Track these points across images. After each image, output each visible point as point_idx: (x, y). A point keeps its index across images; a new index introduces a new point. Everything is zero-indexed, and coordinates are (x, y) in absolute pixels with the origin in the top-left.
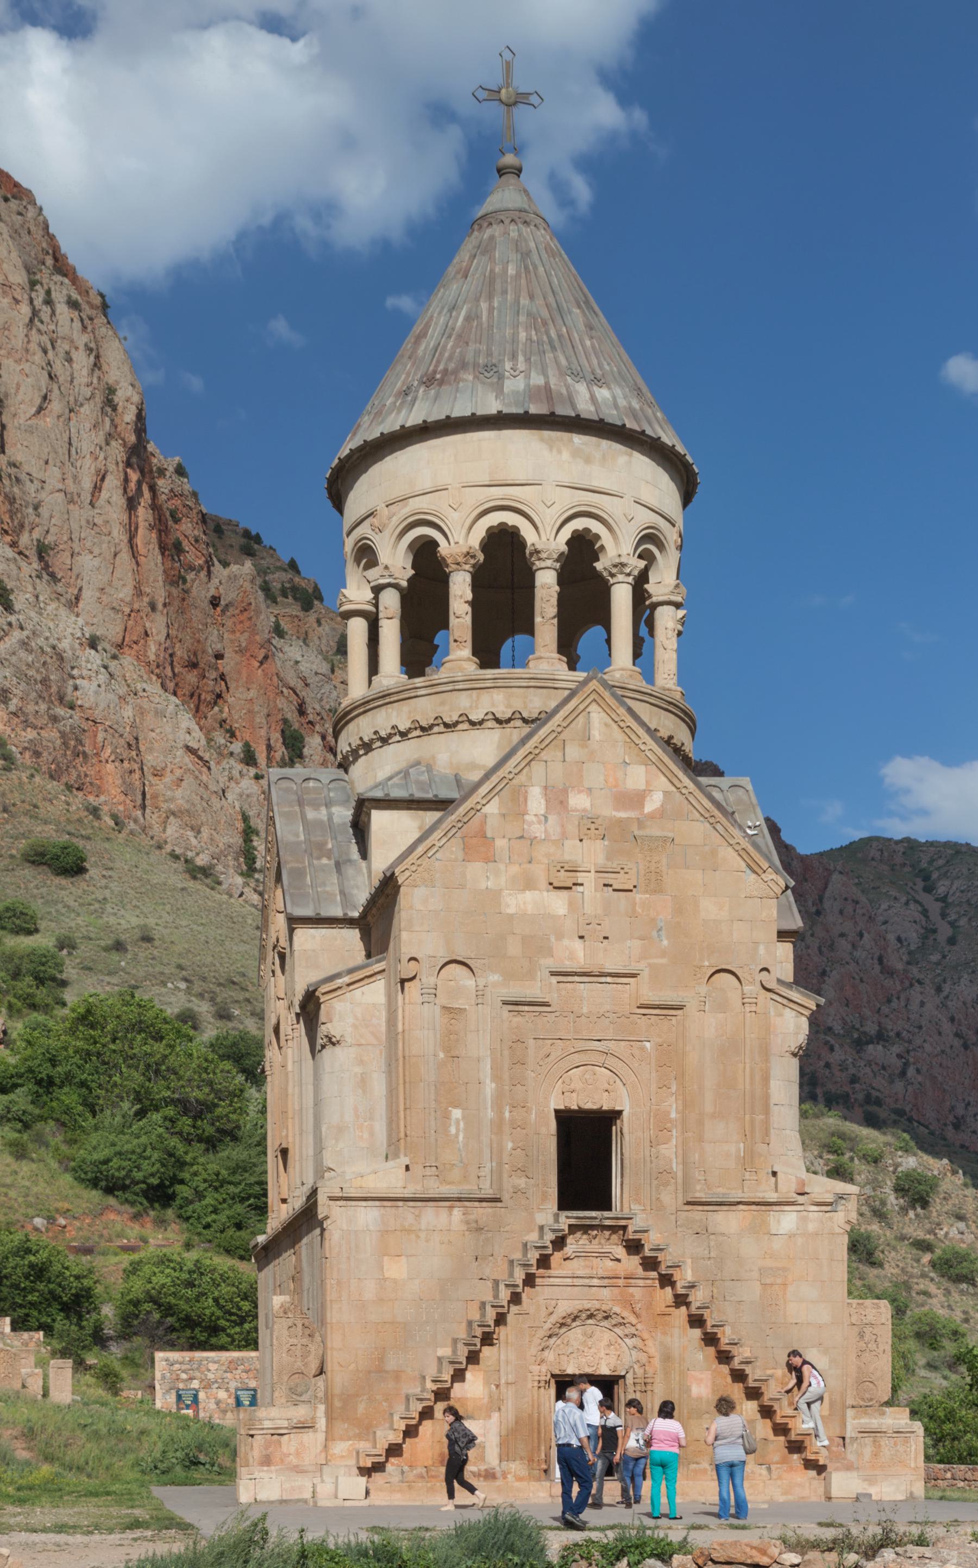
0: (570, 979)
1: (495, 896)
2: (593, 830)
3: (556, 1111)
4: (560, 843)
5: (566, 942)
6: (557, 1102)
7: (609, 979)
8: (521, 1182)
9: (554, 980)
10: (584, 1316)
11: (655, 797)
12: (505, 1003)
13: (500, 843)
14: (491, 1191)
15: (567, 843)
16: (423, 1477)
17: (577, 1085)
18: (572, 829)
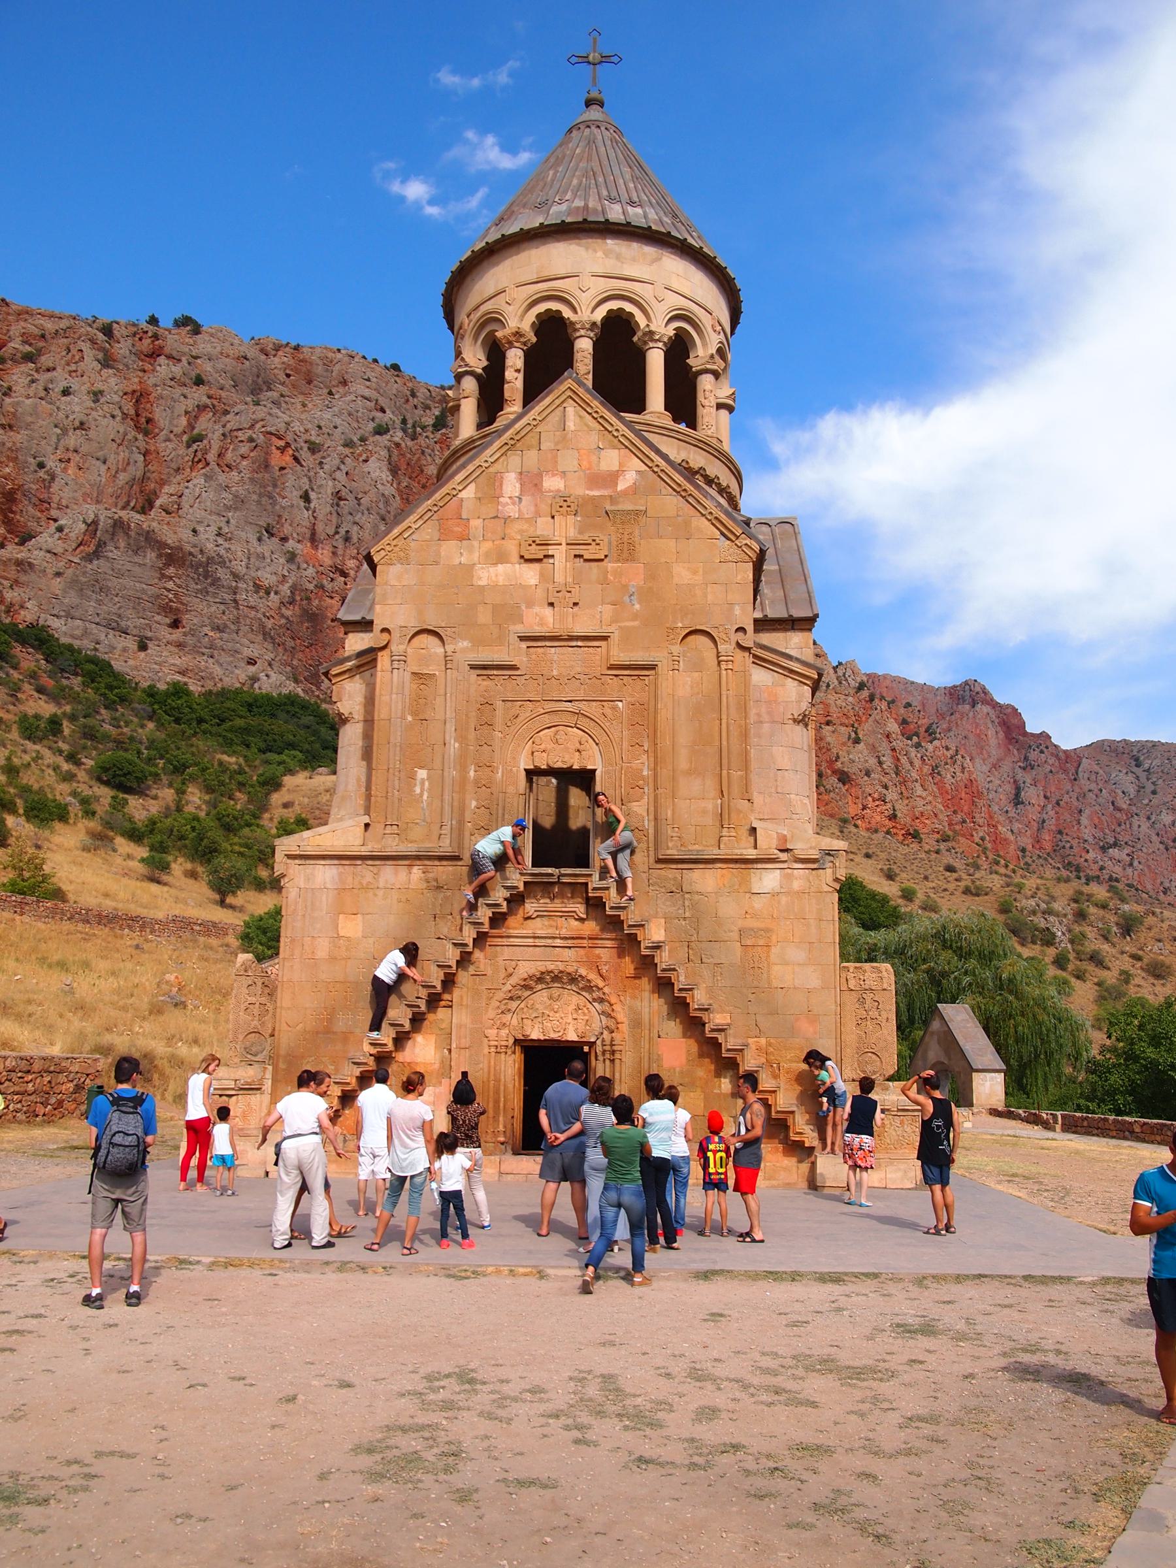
0: (539, 644)
2: (565, 509)
4: (532, 521)
5: (537, 609)
7: (579, 643)
9: (524, 645)
12: (473, 667)
13: (476, 523)
14: (450, 849)
15: (539, 520)
17: (549, 745)
18: (544, 508)
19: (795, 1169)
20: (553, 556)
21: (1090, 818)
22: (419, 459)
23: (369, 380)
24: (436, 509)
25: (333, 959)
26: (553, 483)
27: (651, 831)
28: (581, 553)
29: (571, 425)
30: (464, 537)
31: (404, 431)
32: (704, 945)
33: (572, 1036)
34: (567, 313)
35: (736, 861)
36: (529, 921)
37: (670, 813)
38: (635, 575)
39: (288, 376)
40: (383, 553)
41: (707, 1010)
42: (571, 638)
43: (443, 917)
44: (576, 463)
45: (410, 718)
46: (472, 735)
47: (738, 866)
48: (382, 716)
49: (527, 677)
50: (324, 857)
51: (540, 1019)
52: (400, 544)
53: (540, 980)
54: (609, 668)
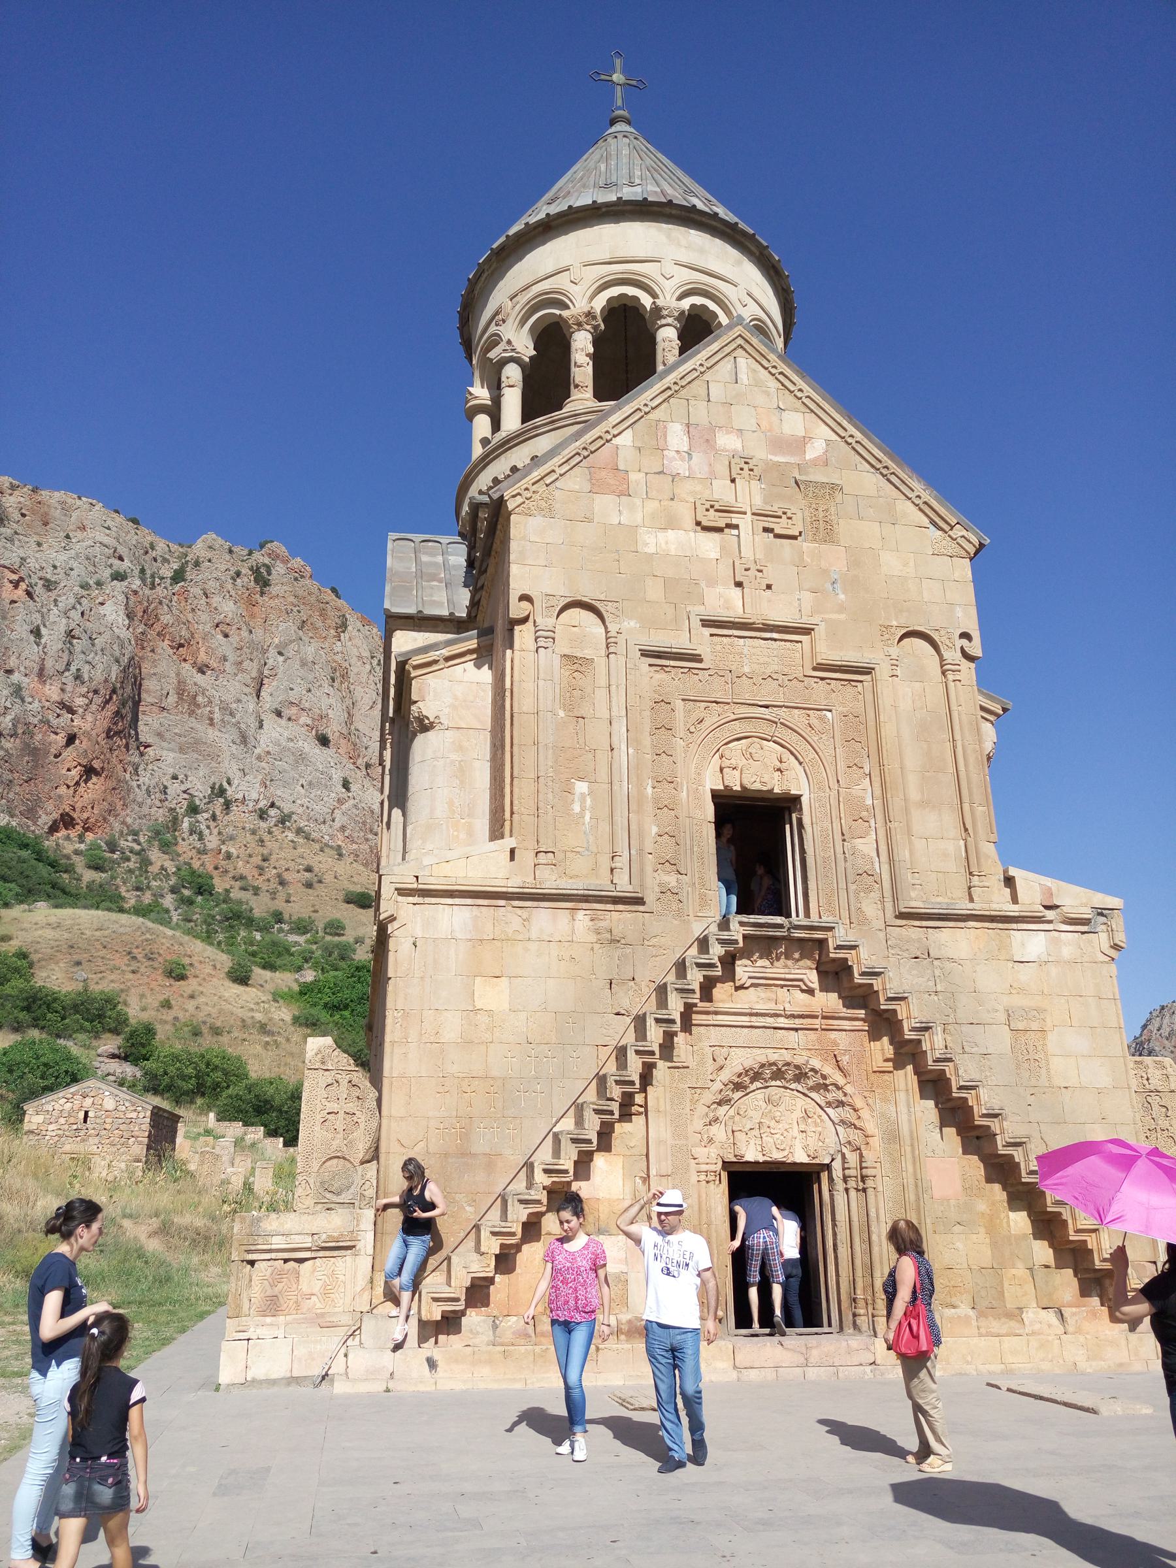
3: (715, 795)
5: (720, 589)
6: (712, 782)
7: (775, 635)
8: (671, 880)
9: (707, 631)
10: (767, 1073)
11: (815, 444)
12: (645, 654)
13: (633, 477)
14: (630, 888)
16: (527, 1336)
17: (742, 762)
19: (1123, 1342)
20: (736, 527)
22: (156, 608)
23: (109, 528)
24: (586, 453)
25: (467, 1043)
26: (728, 442)
27: (886, 877)
28: (771, 526)
29: (743, 377)
31: (143, 580)
32: (965, 1028)
34: (646, 301)
35: (992, 919)
36: (741, 992)
37: (907, 853)
38: (835, 559)
39: (23, 515)
40: (519, 500)
41: (996, 1116)
42: (768, 628)
43: (623, 982)
44: (754, 421)
45: (562, 714)
46: (647, 741)
47: (994, 925)
48: (525, 709)
49: (710, 672)
50: (451, 894)
51: (756, 1132)
52: (541, 491)
53: (757, 1076)
54: (814, 669)
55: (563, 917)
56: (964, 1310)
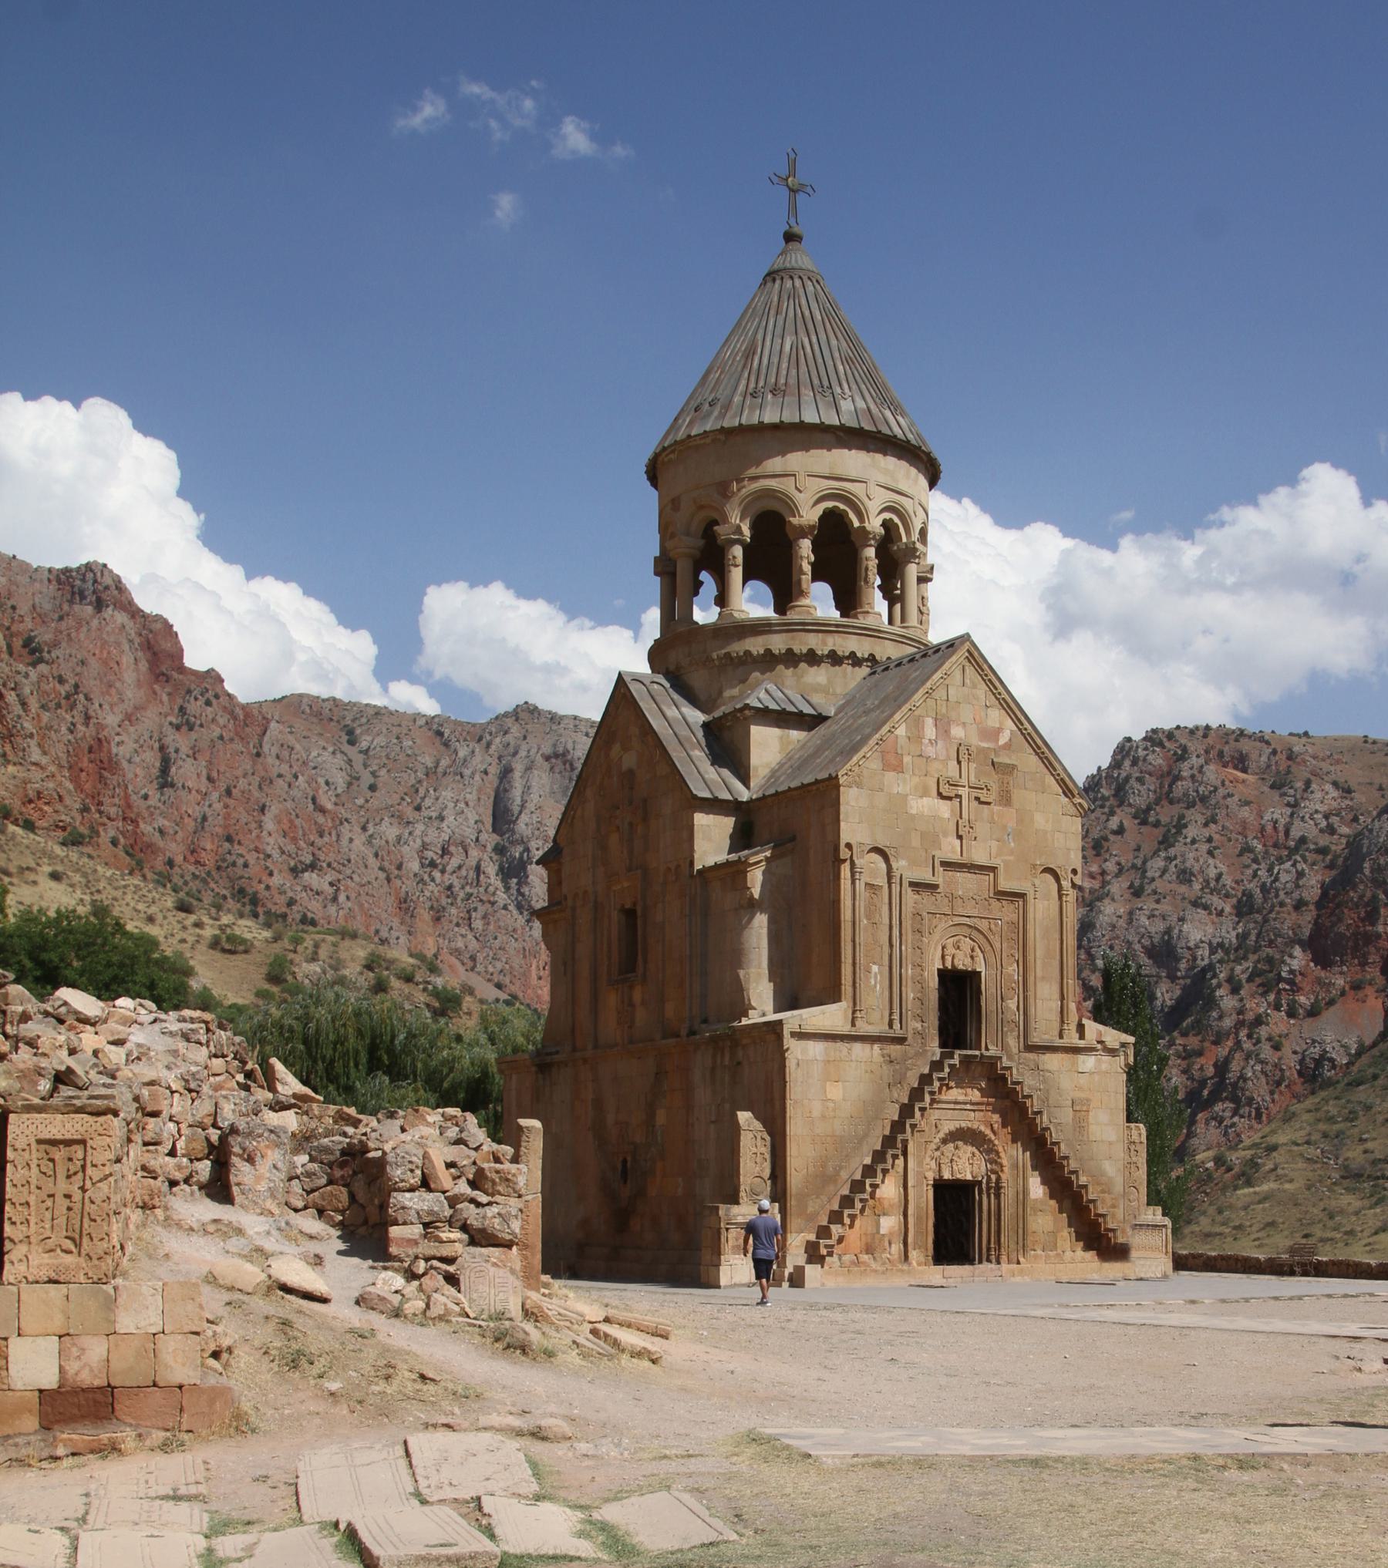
1: (904, 798)
4: (945, 762)
13: (907, 759)
21: (278, 820)
26: (957, 732)
30: (899, 768)
33: (969, 1177)
34: (856, 524)
38: (1009, 817)
55: (867, 1046)
56: (1039, 1252)
